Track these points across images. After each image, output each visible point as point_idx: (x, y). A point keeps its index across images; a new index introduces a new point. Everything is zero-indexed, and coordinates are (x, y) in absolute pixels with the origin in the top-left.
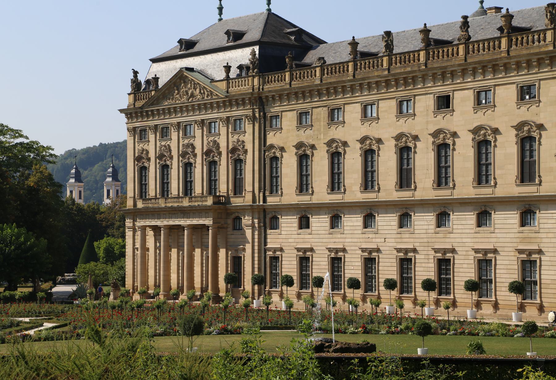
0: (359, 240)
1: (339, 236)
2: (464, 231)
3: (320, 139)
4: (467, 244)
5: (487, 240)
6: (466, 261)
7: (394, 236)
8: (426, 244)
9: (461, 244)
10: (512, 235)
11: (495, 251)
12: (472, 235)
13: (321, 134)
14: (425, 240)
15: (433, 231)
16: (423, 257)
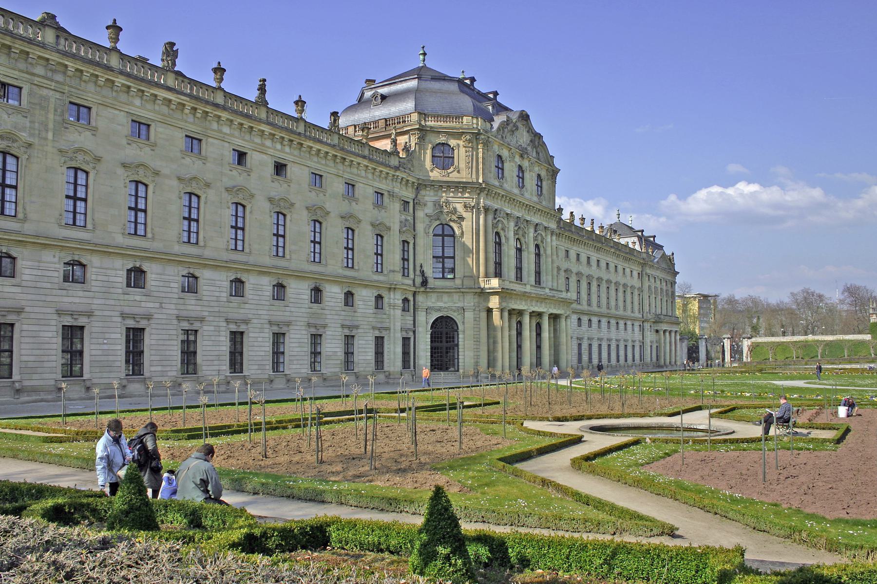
0: (117, 303)
1: (81, 294)
2: (260, 302)
3: (46, 139)
4: (262, 317)
5: (281, 313)
6: (262, 335)
7: (174, 301)
8: (217, 314)
9: (257, 316)
10: (303, 310)
11: (288, 324)
12: (266, 308)
13: (47, 131)
14: (217, 309)
15: (225, 299)
16: (212, 328)
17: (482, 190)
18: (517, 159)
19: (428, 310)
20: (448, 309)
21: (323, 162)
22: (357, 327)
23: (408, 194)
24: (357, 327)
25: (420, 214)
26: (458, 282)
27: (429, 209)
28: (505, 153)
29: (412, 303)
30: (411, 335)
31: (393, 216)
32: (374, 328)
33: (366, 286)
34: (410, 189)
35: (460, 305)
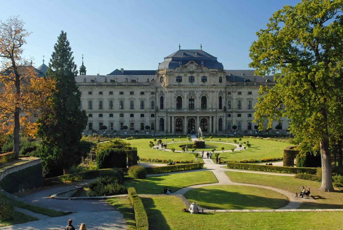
17: (168, 88)
18: (189, 75)
19: (159, 116)
20: (162, 116)
21: (123, 89)
22: (135, 121)
23: (154, 90)
24: (135, 121)
25: (157, 94)
26: (164, 110)
27: (159, 93)
28: (182, 75)
29: (155, 115)
30: (155, 122)
31: (147, 97)
32: (140, 121)
33: (137, 113)
34: (154, 89)
35: (164, 115)
